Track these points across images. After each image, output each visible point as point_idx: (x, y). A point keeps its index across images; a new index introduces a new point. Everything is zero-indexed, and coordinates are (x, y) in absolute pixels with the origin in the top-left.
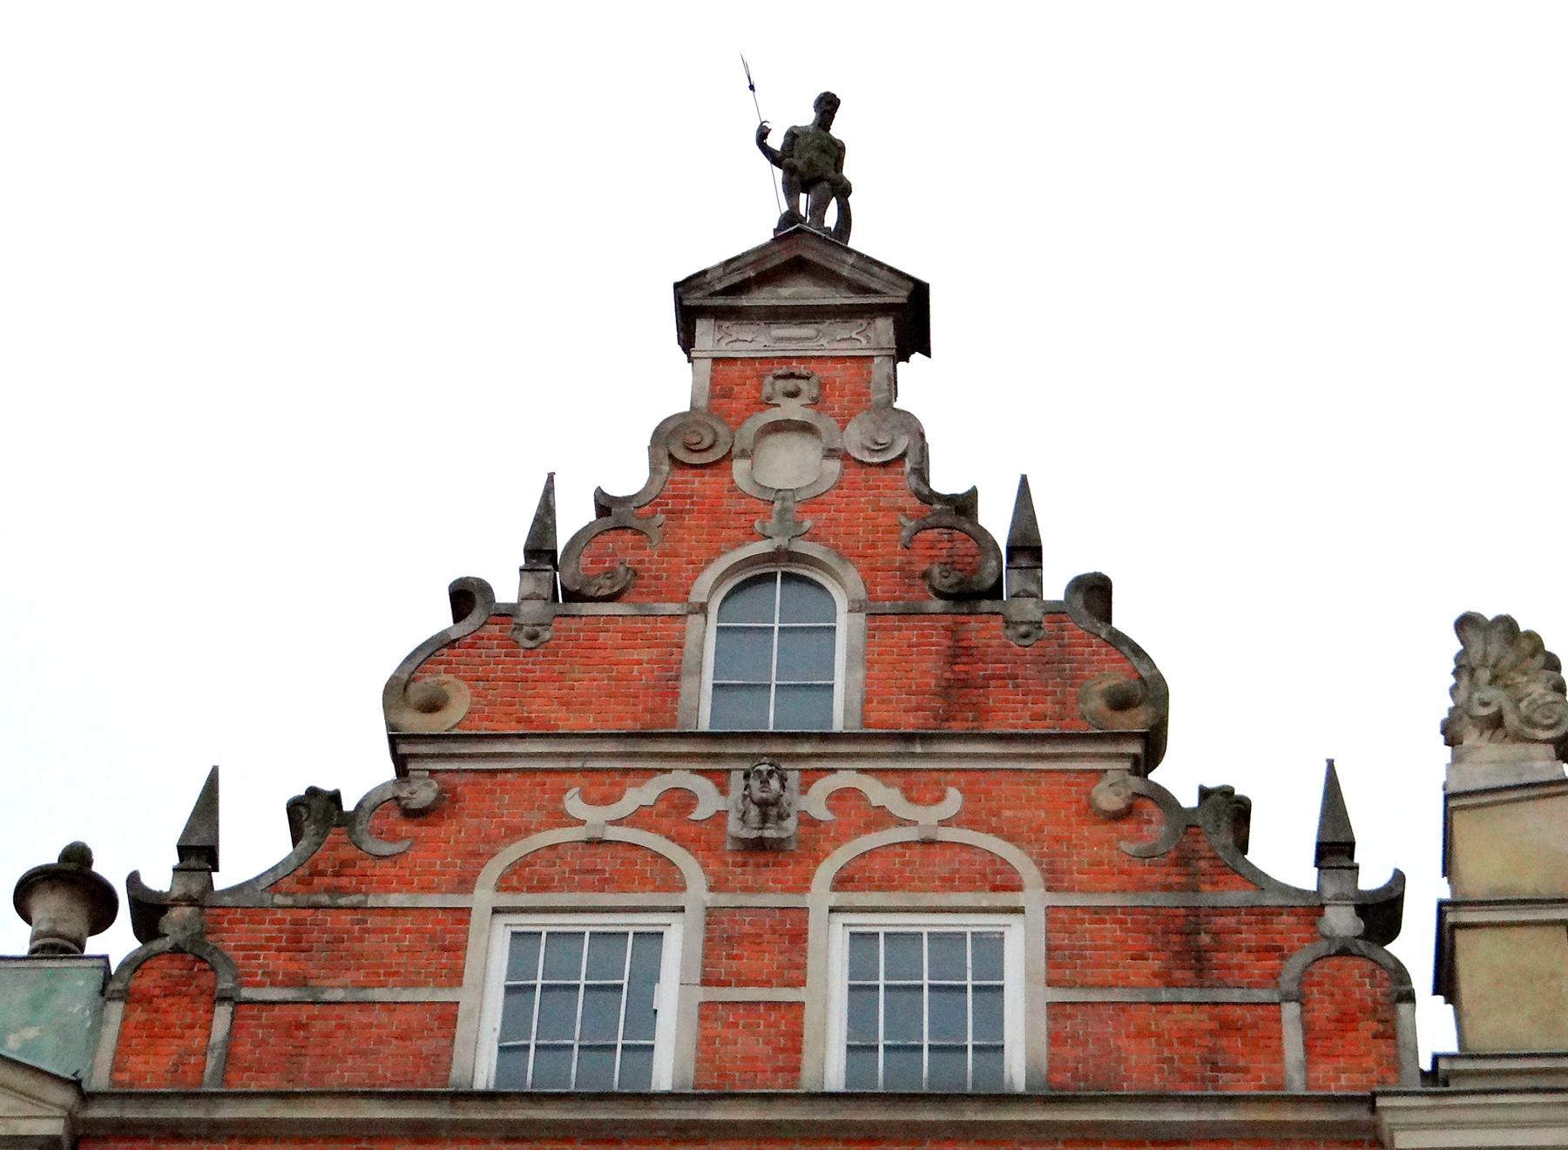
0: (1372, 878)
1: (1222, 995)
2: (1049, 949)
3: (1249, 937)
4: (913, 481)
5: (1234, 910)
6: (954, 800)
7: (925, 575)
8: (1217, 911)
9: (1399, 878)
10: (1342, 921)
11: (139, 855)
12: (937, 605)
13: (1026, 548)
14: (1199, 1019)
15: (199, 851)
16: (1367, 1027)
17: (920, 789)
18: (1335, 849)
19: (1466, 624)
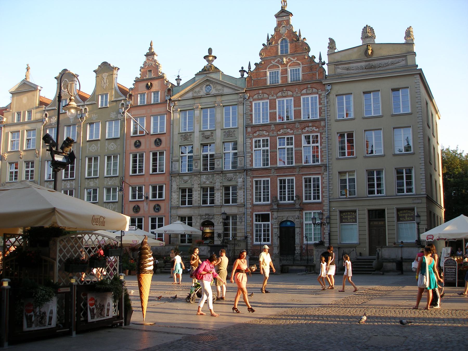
10: (320, 65)
11: (246, 69)
13: (300, 36)
15: (250, 68)
17: (294, 58)
18: (320, 59)
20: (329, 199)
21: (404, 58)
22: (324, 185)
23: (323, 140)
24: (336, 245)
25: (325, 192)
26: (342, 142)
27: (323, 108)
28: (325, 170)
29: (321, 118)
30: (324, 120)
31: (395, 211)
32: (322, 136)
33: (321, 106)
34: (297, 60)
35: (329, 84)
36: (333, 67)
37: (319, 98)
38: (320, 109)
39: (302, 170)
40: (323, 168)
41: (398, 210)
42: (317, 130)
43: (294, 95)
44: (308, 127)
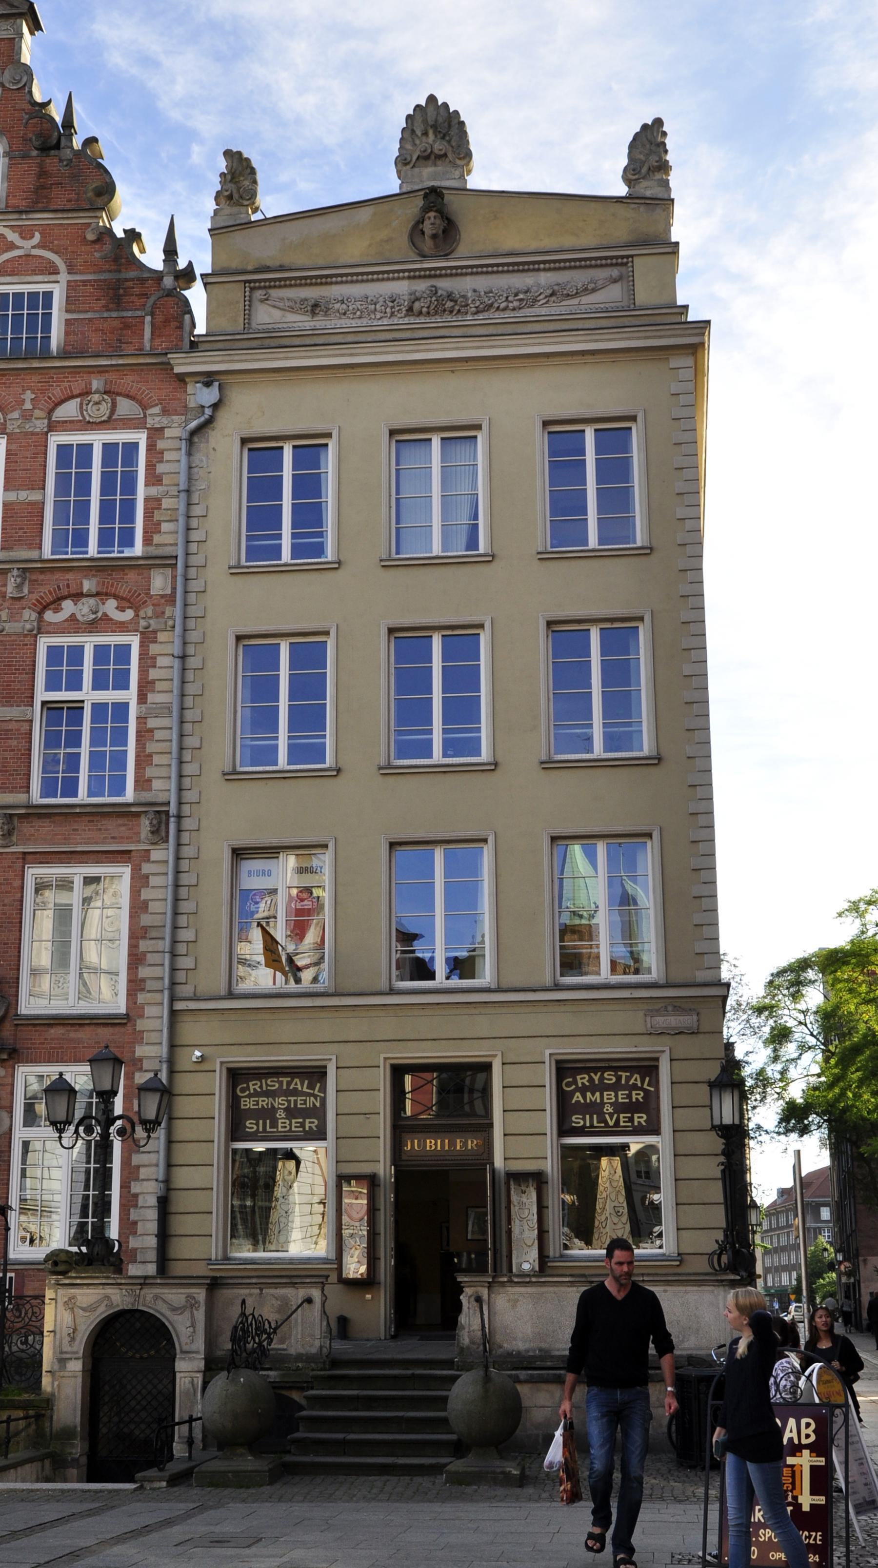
0: (182, 264)
1: (125, 314)
2: (67, 297)
3: (137, 290)
4: (28, 97)
5: (132, 280)
6: (37, 236)
7: (31, 140)
8: (127, 280)
9: (190, 264)
10: (168, 282)
12: (34, 153)
13: (68, 123)
14: (116, 323)
16: (174, 324)
17: (26, 233)
18: (170, 251)
19: (228, 154)
20: (173, 999)
21: (615, 272)
22: (146, 920)
23: (153, 674)
24: (201, 1270)
25: (151, 958)
26: (263, 689)
27: (166, 503)
28: (159, 834)
29: (153, 551)
30: (167, 562)
31: (547, 1075)
32: (154, 649)
33: (154, 491)
34: (41, 246)
35: (208, 379)
36: (237, 293)
37: (151, 447)
38: (153, 505)
39: (26, 828)
40: (145, 825)
41: (564, 1069)
42: (129, 614)
43: (9, 428)
44: (77, 596)
